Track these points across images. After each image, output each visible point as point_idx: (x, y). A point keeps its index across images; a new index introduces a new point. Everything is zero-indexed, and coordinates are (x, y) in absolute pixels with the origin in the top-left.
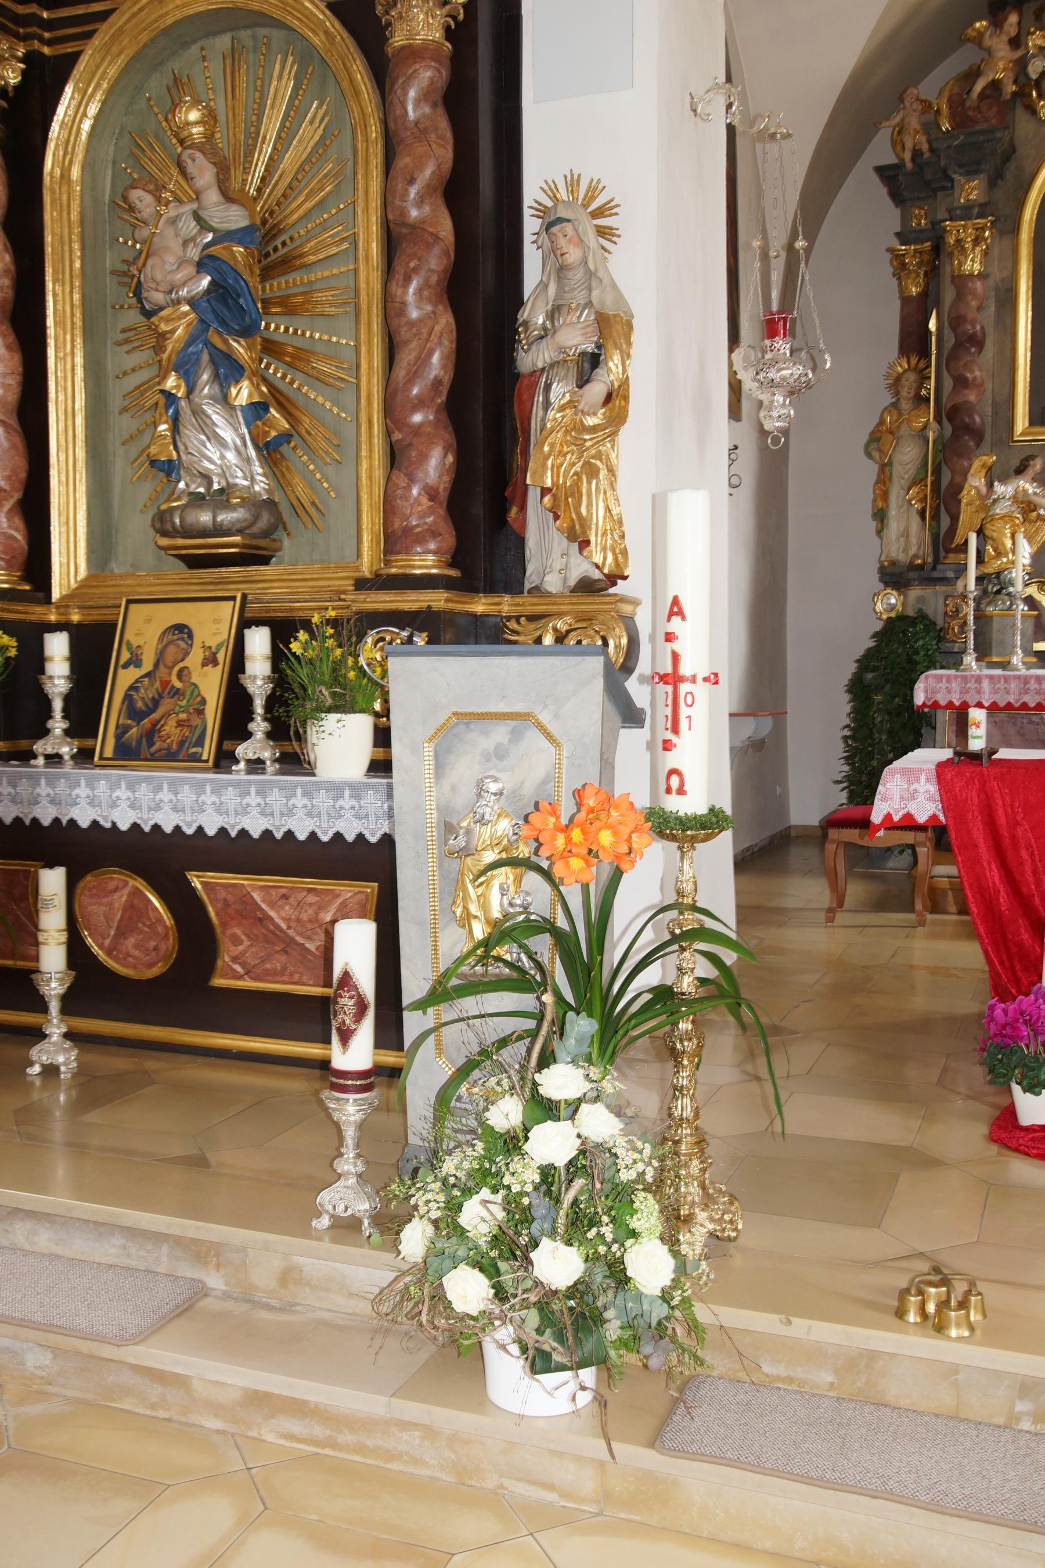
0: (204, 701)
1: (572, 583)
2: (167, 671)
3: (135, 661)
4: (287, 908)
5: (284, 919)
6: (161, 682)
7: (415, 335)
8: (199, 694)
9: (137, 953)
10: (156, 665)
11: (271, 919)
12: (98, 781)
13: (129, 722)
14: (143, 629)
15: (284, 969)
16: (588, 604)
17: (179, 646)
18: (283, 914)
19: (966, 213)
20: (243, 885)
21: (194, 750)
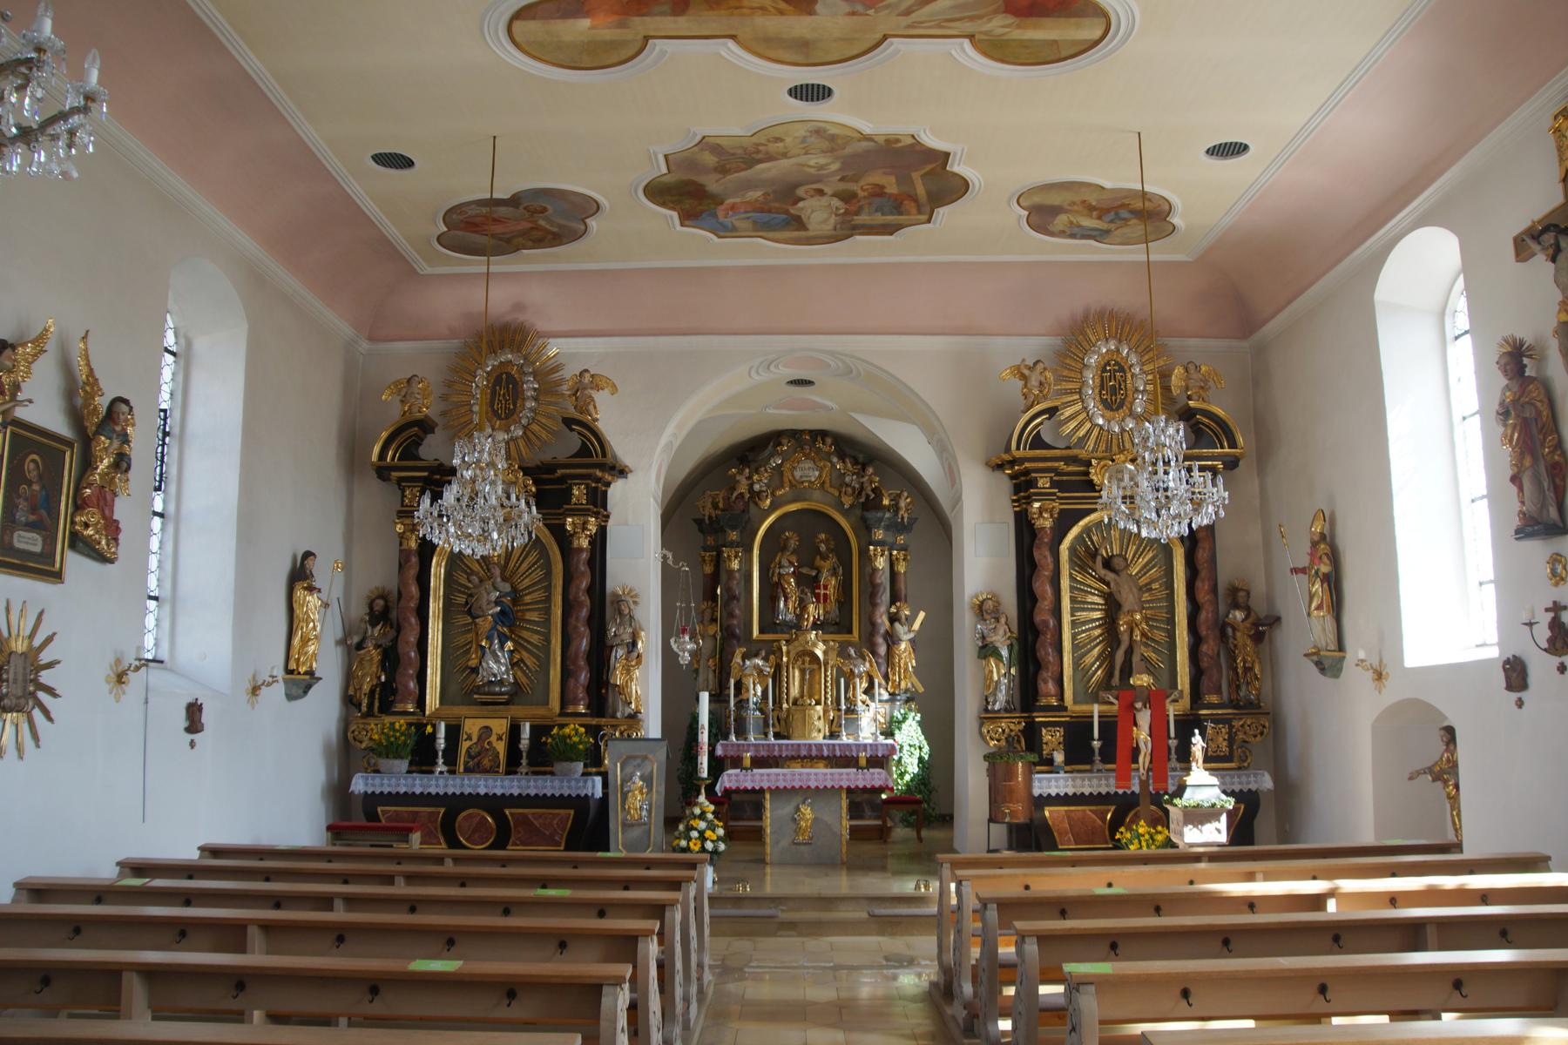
3: (469, 738)
14: (472, 727)
16: (630, 721)
19: (732, 545)
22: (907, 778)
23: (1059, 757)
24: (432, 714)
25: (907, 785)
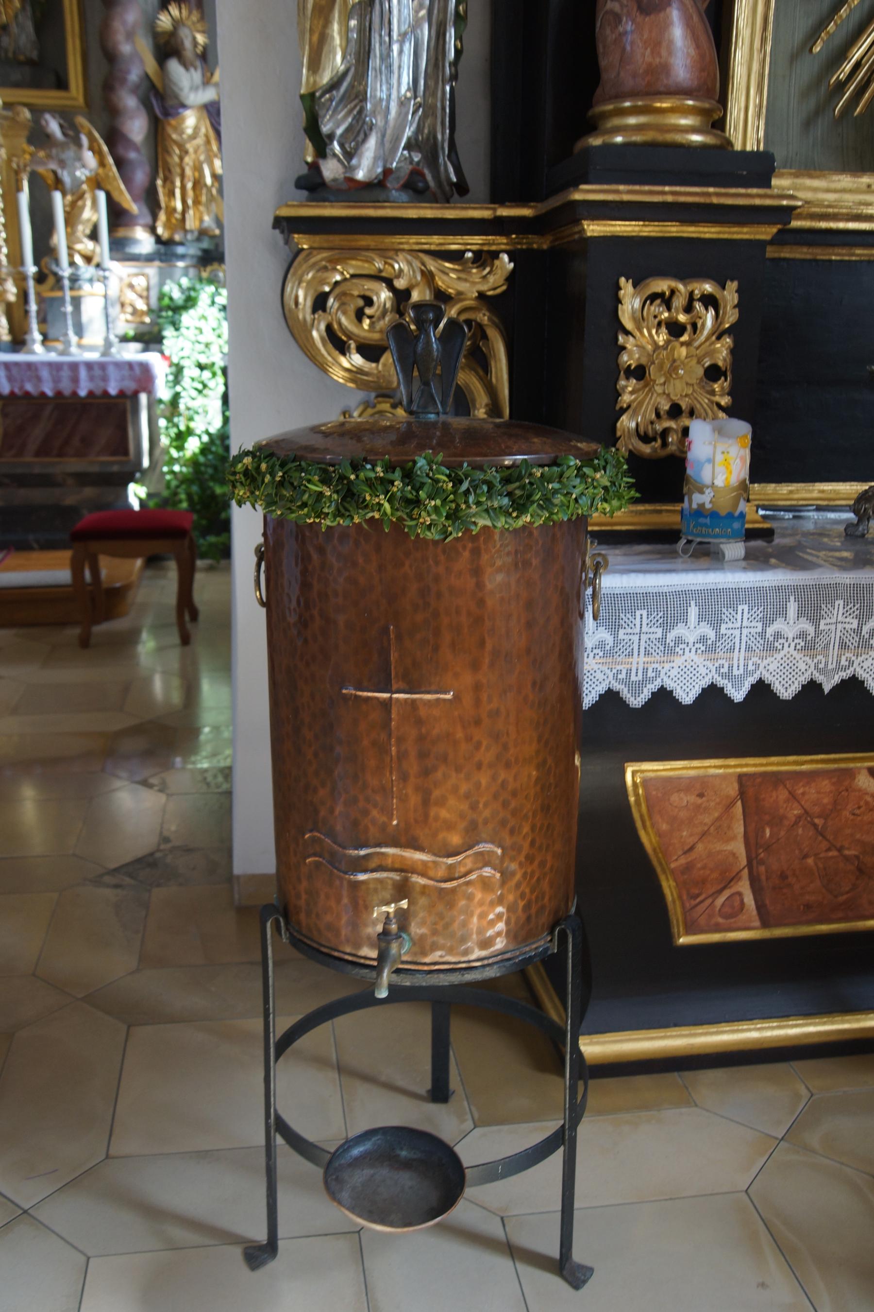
22: (193, 446)
23: (719, 457)
25: (194, 462)
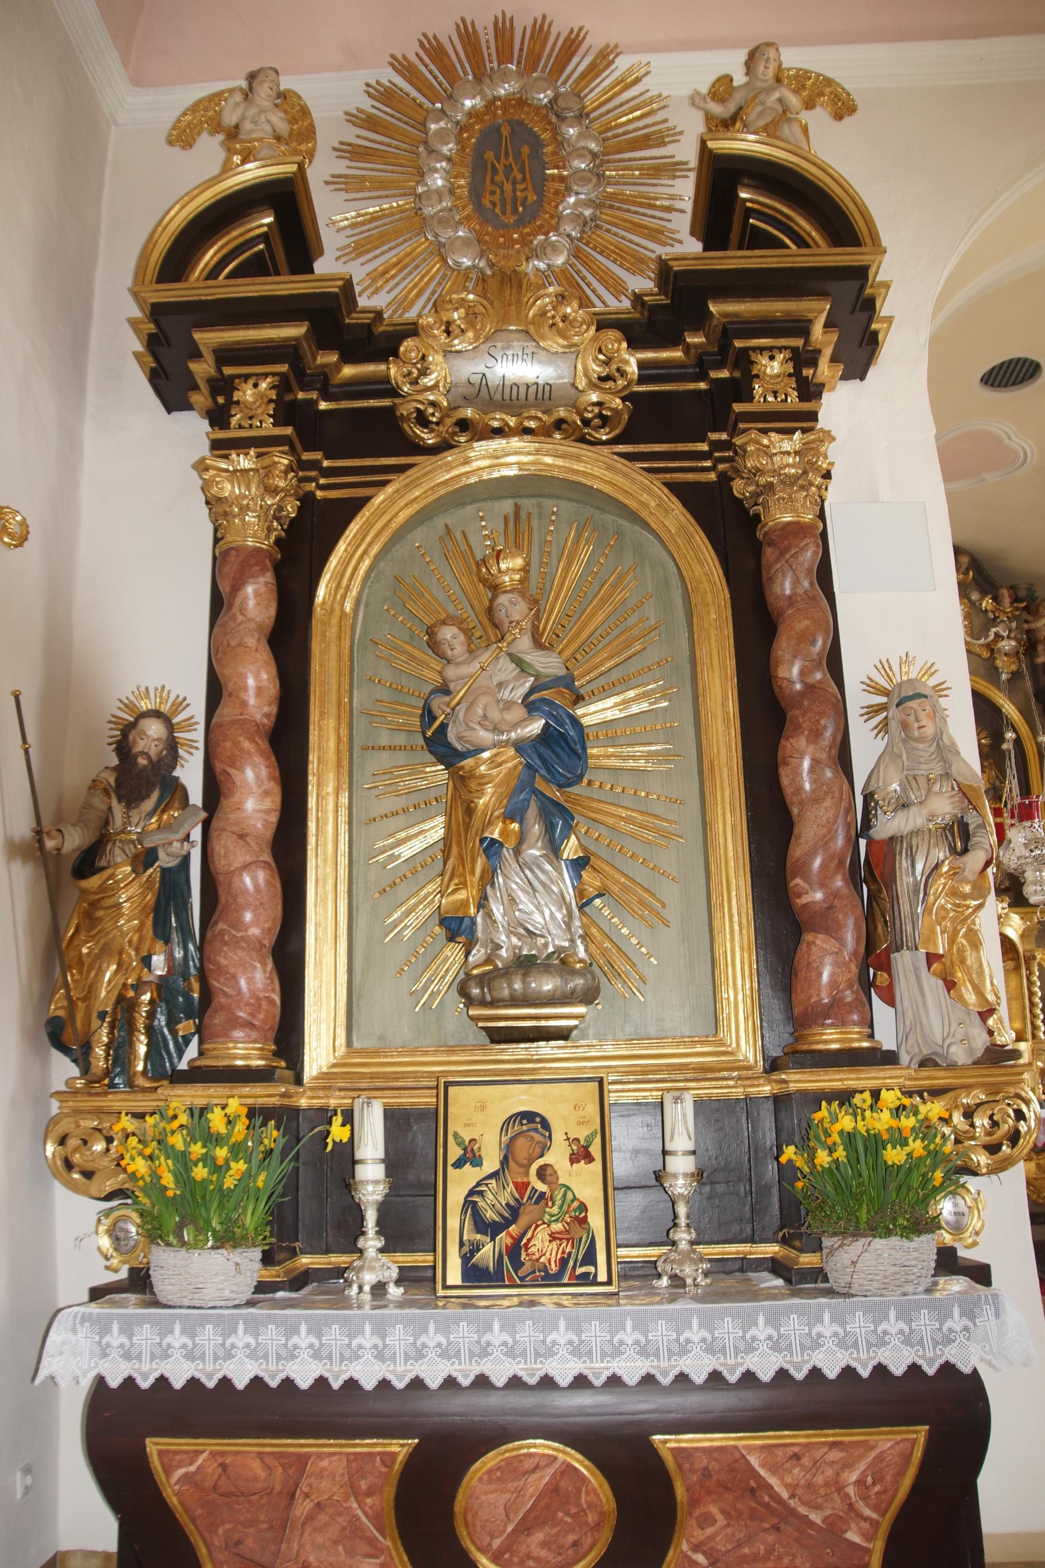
0: (583, 1207)
1: (979, 1054)
2: (522, 1170)
4: (796, 1471)
5: (787, 1486)
6: (516, 1184)
7: (826, 793)
8: (575, 1199)
9: (543, 1553)
10: (505, 1162)
11: (770, 1487)
12: (523, 1322)
13: (479, 1236)
15: (769, 1552)
16: (994, 1075)
17: (532, 1139)
18: (789, 1479)
20: (736, 1447)
21: (584, 1269)
24: (322, 1076)
